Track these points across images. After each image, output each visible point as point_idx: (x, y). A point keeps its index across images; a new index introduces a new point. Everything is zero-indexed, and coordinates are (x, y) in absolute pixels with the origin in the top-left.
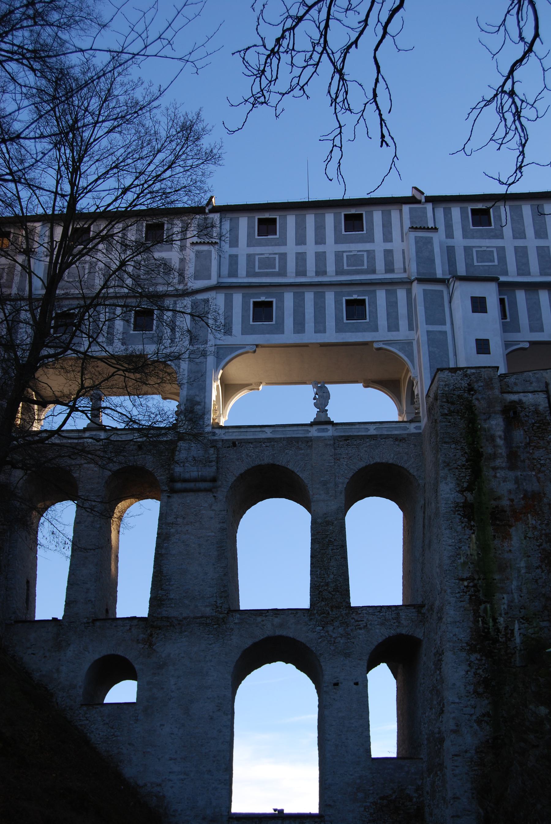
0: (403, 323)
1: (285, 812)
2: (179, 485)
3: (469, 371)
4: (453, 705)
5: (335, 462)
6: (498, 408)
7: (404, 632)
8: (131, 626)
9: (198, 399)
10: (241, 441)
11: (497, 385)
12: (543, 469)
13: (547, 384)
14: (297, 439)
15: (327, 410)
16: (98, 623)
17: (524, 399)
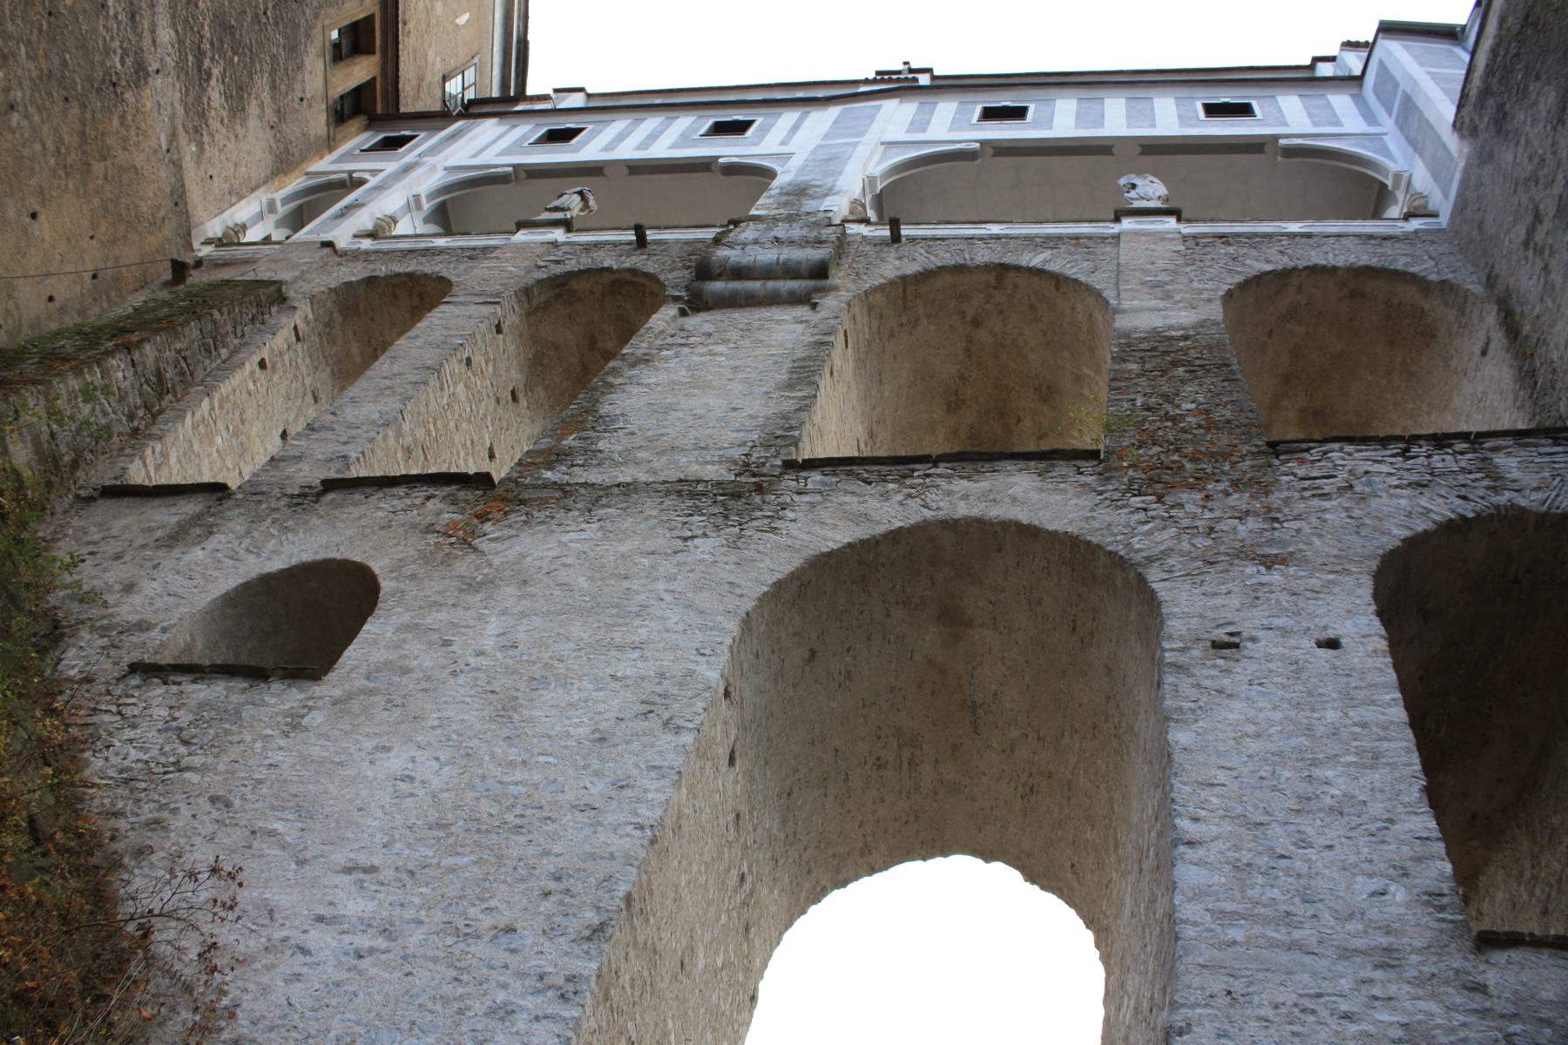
2: (718, 286)
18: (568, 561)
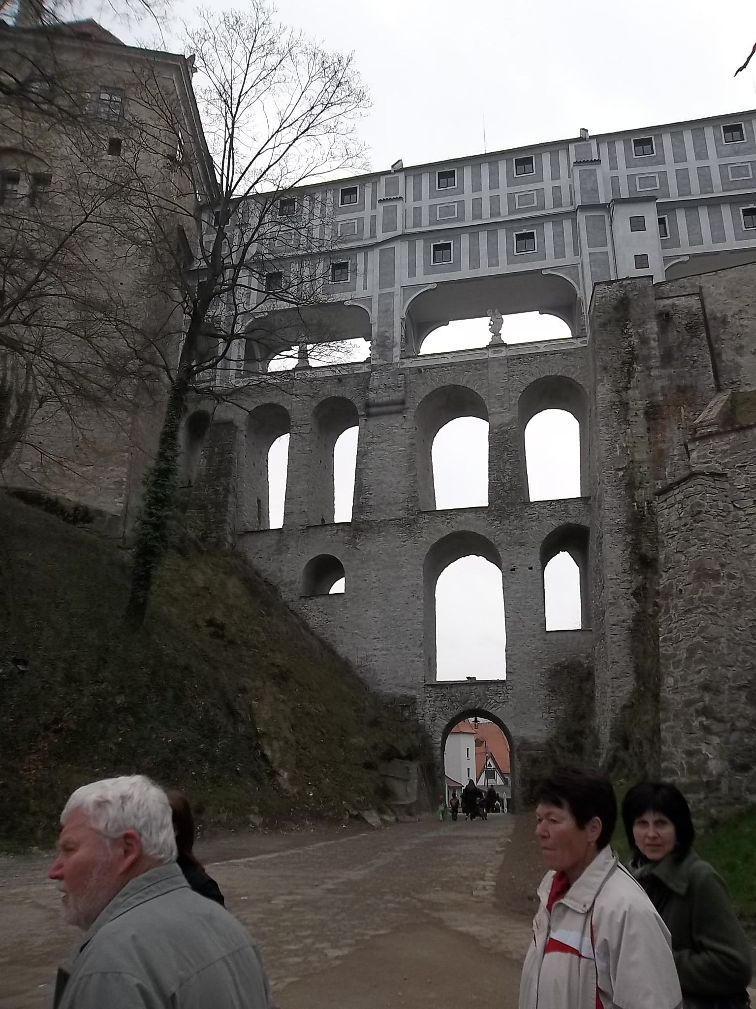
0: (569, 250)
1: (477, 679)
2: (373, 410)
3: (624, 283)
4: (610, 581)
5: (509, 380)
6: (652, 313)
7: (570, 522)
8: (338, 530)
9: (387, 334)
10: (427, 368)
11: (651, 292)
12: (695, 365)
13: (701, 288)
14: (475, 362)
15: (500, 334)
16: (311, 530)
17: (677, 303)
18: (380, 552)
